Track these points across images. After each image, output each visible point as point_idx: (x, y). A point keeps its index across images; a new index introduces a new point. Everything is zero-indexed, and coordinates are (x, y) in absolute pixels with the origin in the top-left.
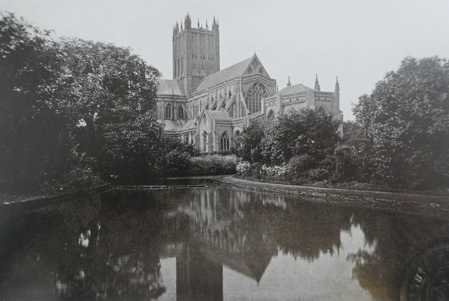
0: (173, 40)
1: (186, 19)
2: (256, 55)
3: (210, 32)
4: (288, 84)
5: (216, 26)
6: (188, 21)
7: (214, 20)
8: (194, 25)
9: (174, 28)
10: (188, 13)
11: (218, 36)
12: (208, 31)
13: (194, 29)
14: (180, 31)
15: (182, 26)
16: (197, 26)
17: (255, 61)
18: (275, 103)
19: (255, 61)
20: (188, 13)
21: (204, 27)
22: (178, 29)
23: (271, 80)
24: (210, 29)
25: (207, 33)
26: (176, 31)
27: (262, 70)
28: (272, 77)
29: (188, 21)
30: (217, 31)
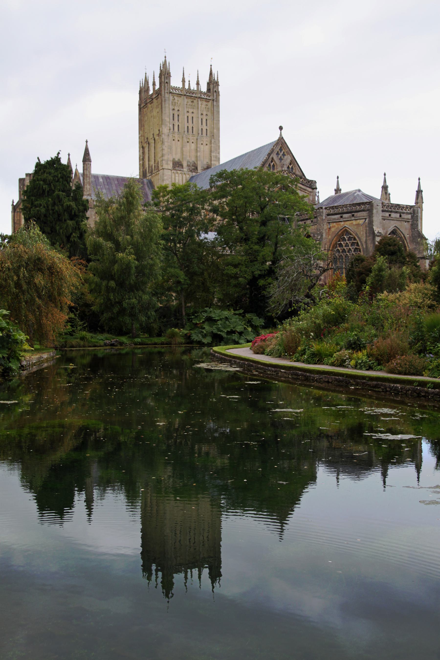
1: (162, 69)
2: (282, 138)
3: (204, 94)
4: (335, 190)
7: (211, 71)
9: (141, 86)
10: (165, 57)
12: (201, 92)
13: (176, 89)
14: (151, 92)
15: (154, 84)
16: (181, 83)
20: (165, 57)
21: (194, 87)
23: (309, 182)
24: (204, 88)
26: (143, 91)
28: (309, 177)
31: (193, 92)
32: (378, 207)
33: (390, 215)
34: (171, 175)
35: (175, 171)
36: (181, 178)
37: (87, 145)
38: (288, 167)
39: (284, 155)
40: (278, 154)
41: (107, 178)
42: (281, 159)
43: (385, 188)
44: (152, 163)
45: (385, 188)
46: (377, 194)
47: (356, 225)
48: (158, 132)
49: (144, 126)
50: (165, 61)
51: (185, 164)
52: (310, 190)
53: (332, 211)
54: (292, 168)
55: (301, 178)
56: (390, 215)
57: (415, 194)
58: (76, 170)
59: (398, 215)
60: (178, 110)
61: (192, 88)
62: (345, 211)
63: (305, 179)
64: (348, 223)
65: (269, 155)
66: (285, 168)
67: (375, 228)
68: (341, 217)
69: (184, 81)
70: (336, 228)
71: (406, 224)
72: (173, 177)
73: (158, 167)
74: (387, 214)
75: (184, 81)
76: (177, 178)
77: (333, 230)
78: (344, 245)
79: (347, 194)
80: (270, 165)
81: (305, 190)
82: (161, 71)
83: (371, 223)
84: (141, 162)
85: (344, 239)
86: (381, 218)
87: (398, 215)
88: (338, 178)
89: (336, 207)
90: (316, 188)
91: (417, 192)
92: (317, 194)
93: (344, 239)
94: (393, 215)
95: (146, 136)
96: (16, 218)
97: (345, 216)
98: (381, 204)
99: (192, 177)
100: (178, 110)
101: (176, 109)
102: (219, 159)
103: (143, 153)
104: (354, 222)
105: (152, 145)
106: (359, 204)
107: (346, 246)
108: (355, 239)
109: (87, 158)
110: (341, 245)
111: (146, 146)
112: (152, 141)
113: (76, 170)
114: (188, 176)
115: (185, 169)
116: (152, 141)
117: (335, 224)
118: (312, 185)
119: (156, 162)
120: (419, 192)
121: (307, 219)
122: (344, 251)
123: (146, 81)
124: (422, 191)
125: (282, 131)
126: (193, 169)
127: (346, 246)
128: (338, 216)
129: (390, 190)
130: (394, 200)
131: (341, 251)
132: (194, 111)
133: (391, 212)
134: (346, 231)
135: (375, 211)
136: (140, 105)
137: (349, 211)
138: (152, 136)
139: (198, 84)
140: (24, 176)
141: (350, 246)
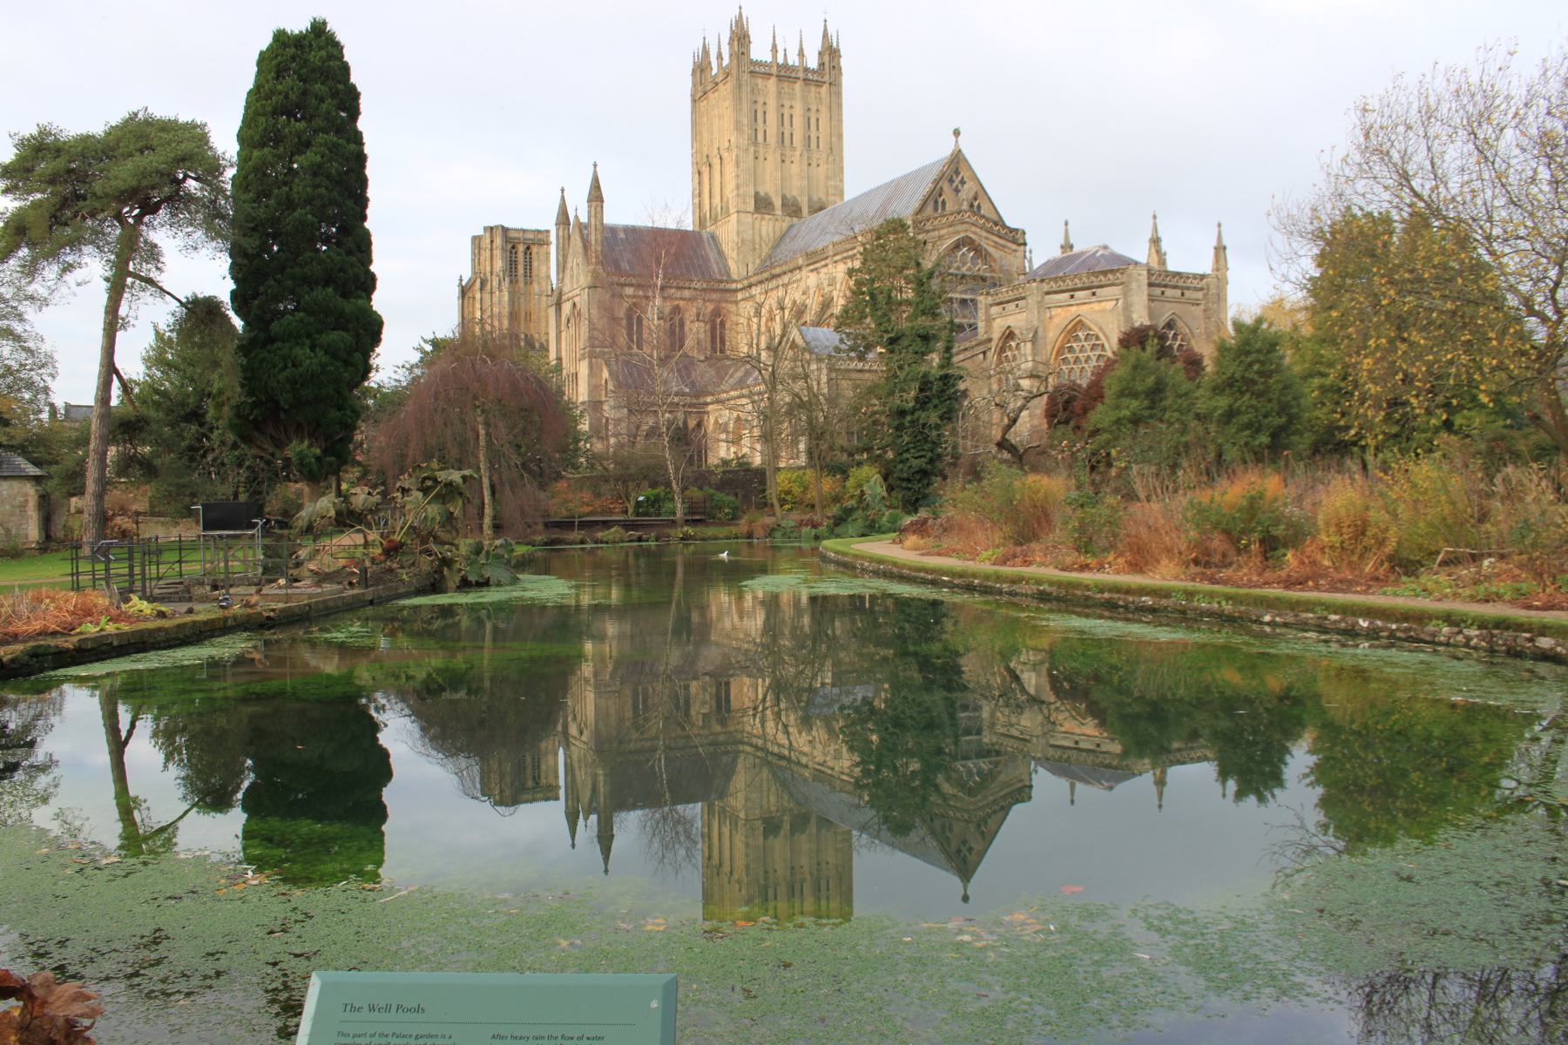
0: (694, 101)
3: (814, 71)
4: (1062, 247)
5: (830, 53)
6: (740, 37)
8: (759, 51)
11: (835, 85)
12: (806, 70)
14: (715, 71)
15: (720, 57)
17: (956, 168)
18: (1021, 303)
19: (956, 168)
21: (793, 60)
22: (710, 63)
24: (813, 63)
25: (801, 75)
26: (701, 68)
27: (980, 194)
29: (740, 37)
30: (836, 69)
31: (793, 68)
32: (1141, 278)
33: (1163, 293)
34: (753, 224)
35: (759, 216)
36: (771, 229)
37: (595, 172)
38: (971, 206)
39: (963, 182)
40: (951, 181)
41: (633, 232)
42: (957, 191)
43: (1156, 241)
44: (717, 201)
45: (1156, 241)
46: (1140, 252)
47: (1101, 311)
48: (727, 145)
49: (701, 133)
50: (740, 14)
51: (777, 202)
52: (1014, 247)
53: (1054, 286)
54: (979, 207)
55: (996, 225)
56: (1163, 293)
57: (1212, 252)
58: (576, 217)
59: (1179, 292)
60: (765, 103)
61: (790, 63)
62: (1079, 286)
63: (1004, 226)
64: (1085, 307)
65: (936, 182)
66: (965, 206)
67: (1134, 316)
68: (1072, 297)
69: (774, 49)
70: (1061, 317)
71: (1193, 308)
72: (757, 226)
73: (728, 208)
74: (1158, 291)
75: (774, 49)
76: (764, 229)
77: (1056, 321)
78: (1077, 349)
79: (1082, 253)
80: (936, 202)
81: (1005, 247)
82: (732, 32)
83: (1127, 308)
84: (697, 201)
85: (1077, 339)
86: (1145, 298)
87: (1179, 292)
88: (1066, 224)
89: (1063, 279)
90: (1025, 244)
91: (1216, 248)
92: (1028, 254)
93: (1077, 339)
94: (1169, 292)
95: (705, 153)
96: (466, 310)
97: (1077, 294)
98: (1145, 273)
99: (792, 226)
100: (765, 103)
101: (761, 100)
102: (841, 193)
103: (700, 183)
104: (1096, 307)
105: (717, 168)
106: (1105, 273)
107: (1081, 351)
108: (1098, 338)
109: (596, 196)
110: (1071, 349)
111: (705, 170)
112: (716, 162)
113: (576, 217)
114: (785, 225)
115: (779, 212)
116: (716, 162)
117: (1059, 310)
118: (1016, 238)
119: (725, 199)
120: (1220, 250)
121: (1008, 302)
122: (1077, 360)
123: (706, 52)
124: (1225, 248)
125: (960, 138)
126: (796, 212)
127: (1081, 351)
128: (1067, 295)
129: (1164, 246)
130: (1172, 266)
131: (1072, 360)
132: (793, 103)
133: (1165, 286)
134: (1079, 324)
135: (1134, 285)
136: (693, 96)
137: (1087, 285)
138: (716, 152)
139: (801, 54)
140: (481, 232)
141: (1088, 348)
